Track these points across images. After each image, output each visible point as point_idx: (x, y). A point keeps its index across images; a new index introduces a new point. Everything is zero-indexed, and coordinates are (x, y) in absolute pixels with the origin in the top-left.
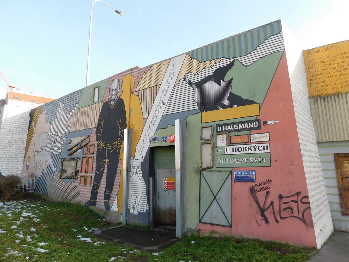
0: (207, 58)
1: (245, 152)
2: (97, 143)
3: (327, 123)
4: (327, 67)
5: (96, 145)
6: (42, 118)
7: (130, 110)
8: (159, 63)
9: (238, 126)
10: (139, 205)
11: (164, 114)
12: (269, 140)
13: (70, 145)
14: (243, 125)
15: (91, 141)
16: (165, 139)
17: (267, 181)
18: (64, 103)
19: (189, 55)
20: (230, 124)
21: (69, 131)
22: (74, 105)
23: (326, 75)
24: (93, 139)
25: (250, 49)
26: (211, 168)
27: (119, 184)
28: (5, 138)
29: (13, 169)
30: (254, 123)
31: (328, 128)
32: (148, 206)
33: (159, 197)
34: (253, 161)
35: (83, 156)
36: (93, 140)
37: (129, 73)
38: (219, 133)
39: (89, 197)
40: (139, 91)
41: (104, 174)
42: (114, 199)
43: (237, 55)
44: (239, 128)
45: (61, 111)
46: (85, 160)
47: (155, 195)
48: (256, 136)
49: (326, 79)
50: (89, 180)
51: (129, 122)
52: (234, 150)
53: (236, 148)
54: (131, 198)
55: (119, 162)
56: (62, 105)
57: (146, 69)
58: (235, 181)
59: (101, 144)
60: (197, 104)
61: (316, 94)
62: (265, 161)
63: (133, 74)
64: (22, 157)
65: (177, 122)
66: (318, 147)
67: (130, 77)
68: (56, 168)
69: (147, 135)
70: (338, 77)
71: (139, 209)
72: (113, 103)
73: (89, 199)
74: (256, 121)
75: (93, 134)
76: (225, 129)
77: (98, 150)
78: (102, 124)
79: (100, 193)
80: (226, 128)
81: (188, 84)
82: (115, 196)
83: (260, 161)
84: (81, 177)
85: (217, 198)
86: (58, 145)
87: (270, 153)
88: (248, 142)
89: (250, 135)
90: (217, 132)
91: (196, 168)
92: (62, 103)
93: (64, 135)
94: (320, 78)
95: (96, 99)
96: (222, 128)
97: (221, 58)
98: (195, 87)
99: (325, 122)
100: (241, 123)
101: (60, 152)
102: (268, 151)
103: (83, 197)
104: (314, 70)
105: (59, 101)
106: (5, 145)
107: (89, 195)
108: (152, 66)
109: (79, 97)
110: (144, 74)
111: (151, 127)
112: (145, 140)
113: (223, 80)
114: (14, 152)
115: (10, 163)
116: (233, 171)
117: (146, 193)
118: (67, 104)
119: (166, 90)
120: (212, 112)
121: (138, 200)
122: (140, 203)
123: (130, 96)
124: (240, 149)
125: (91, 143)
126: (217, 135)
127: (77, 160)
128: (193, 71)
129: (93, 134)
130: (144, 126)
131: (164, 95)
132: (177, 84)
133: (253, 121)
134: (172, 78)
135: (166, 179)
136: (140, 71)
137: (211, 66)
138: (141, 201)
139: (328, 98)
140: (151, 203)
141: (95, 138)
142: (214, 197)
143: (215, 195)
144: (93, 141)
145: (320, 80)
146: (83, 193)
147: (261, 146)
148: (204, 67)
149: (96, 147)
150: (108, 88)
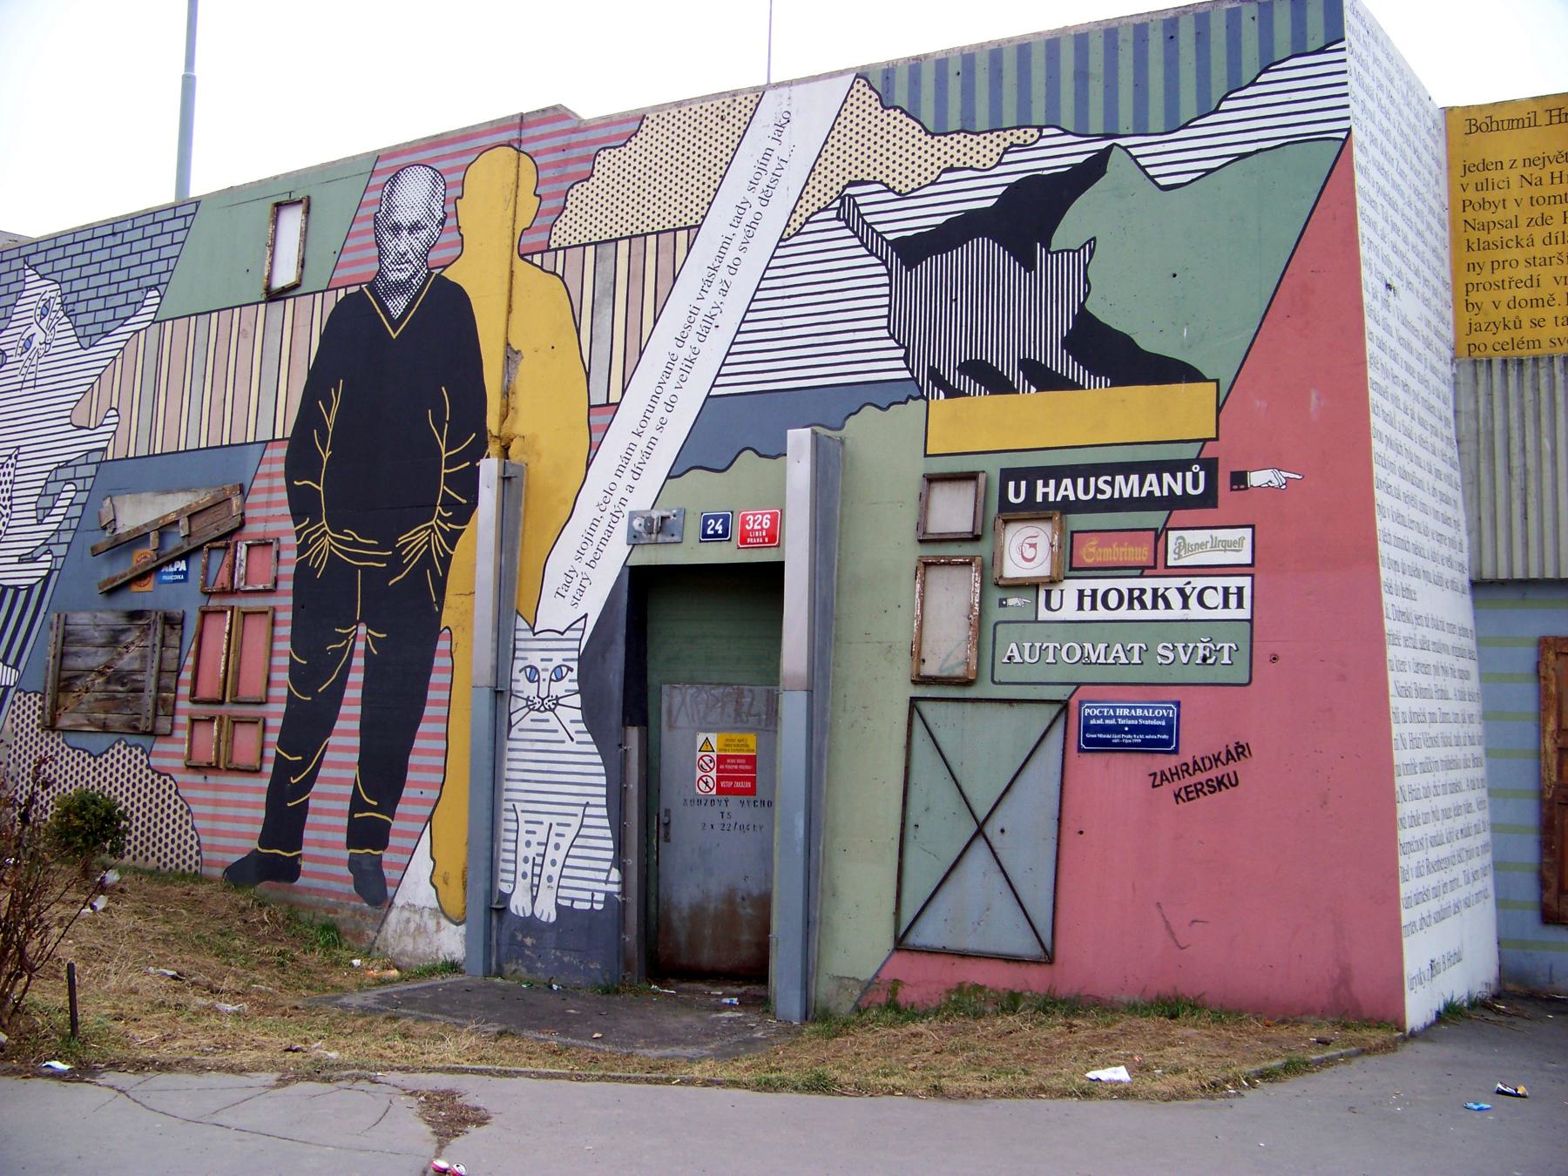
1: (1137, 613)
2: (299, 534)
3: (1525, 490)
4: (1548, 210)
5: (291, 540)
7: (511, 356)
8: (695, 107)
9: (1111, 484)
10: (566, 872)
11: (715, 391)
12: (1249, 562)
14: (1134, 478)
15: (254, 519)
16: (720, 528)
17: (1228, 752)
18: (57, 277)
19: (871, 88)
20: (1074, 472)
21: (104, 450)
23: (1539, 251)
24: (268, 504)
25: (1188, 109)
27: (440, 761)
30: (1189, 475)
31: (1525, 516)
32: (615, 875)
33: (667, 834)
34: (1171, 656)
38: (1010, 514)
39: (250, 836)
40: (565, 248)
41: (344, 710)
42: (410, 843)
43: (1125, 121)
44: (1116, 495)
48: (1193, 537)
51: (504, 417)
52: (1087, 601)
53: (1094, 592)
54: (512, 836)
55: (442, 645)
56: (38, 290)
57: (615, 130)
58: (1080, 750)
59: (325, 533)
60: (903, 351)
62: (1226, 660)
65: (799, 440)
66: (1475, 601)
67: (514, 164)
68: (15, 666)
69: (615, 499)
71: (562, 892)
72: (397, 305)
73: (255, 845)
74: (1196, 468)
75: (270, 476)
76: (1045, 495)
77: (303, 572)
78: (330, 422)
79: (319, 811)
80: (1051, 489)
81: (861, 239)
83: (1205, 659)
85: (991, 830)
87: (1251, 621)
88: (1156, 566)
89: (1166, 529)
90: (1004, 504)
92: (43, 277)
93: (67, 473)
94: (1514, 263)
96: (1031, 491)
97: (1040, 129)
99: (1516, 485)
100: (1126, 469)
101: (44, 573)
102: (1245, 613)
103: (214, 833)
104: (1485, 216)
107: (254, 820)
108: (652, 116)
109: (166, 253)
110: (597, 154)
111: (636, 457)
112: (603, 526)
113: (1046, 244)
116: (1074, 702)
117: (604, 812)
118: (80, 285)
119: (728, 260)
120: (983, 404)
121: (557, 847)
122: (569, 862)
123: (512, 272)
124: (1113, 599)
125: (254, 529)
126: (1006, 522)
128: (886, 172)
130: (593, 448)
132: (798, 234)
133: (1184, 465)
134: (765, 200)
135: (713, 738)
136: (575, 138)
137: (986, 160)
138: (573, 852)
139: (1541, 365)
140: (632, 862)
141: (279, 504)
142: (974, 828)
143: (981, 814)
146: (209, 810)
147: (1215, 589)
148: (953, 161)
149: (290, 555)
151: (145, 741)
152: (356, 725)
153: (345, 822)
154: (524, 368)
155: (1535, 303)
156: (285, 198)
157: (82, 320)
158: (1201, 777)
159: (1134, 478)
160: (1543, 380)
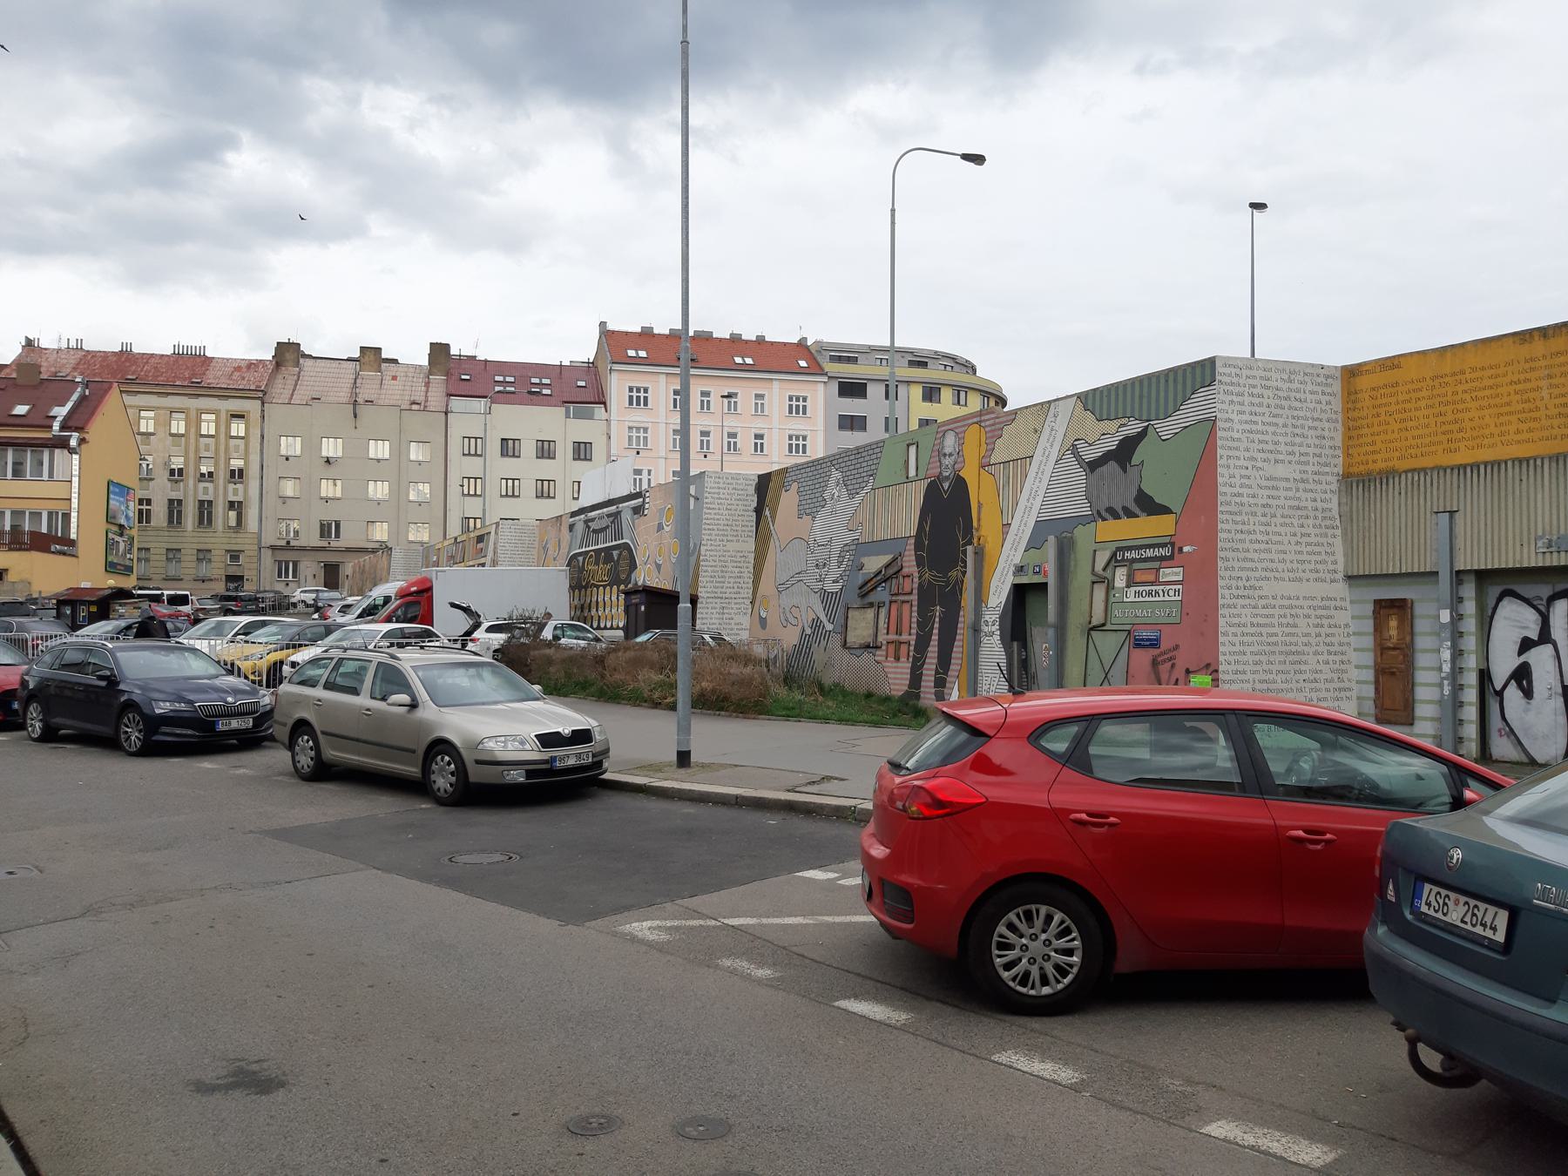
0: (1109, 414)
1: (1151, 599)
5: (916, 575)
6: (788, 502)
7: (980, 506)
9: (1145, 552)
13: (861, 572)
14: (1152, 550)
18: (841, 470)
21: (858, 539)
22: (866, 479)
23: (1376, 429)
24: (910, 561)
26: (1104, 625)
28: (712, 553)
29: (733, 626)
35: (890, 598)
36: (910, 564)
37: (975, 420)
45: (834, 490)
46: (894, 606)
47: (1027, 678)
49: (1377, 437)
50: (904, 648)
55: (961, 613)
56: (836, 475)
61: (1355, 470)
63: (983, 424)
64: (746, 596)
66: (1350, 586)
68: (833, 623)
70: (1396, 435)
72: (946, 485)
73: (906, 688)
75: (910, 550)
77: (920, 586)
78: (928, 529)
82: (953, 679)
84: (888, 643)
86: (834, 572)
88: (1156, 582)
91: (1082, 626)
93: (846, 548)
95: (912, 473)
97: (1129, 418)
98: (1088, 470)
102: (1180, 598)
103: (895, 684)
104: (1356, 414)
105: (829, 464)
106: (712, 569)
107: (906, 679)
114: (731, 585)
115: (725, 611)
118: (849, 473)
120: (1111, 522)
125: (905, 571)
126: (1116, 567)
127: (879, 607)
129: (910, 550)
130: (1004, 540)
131: (1038, 480)
138: (998, 687)
141: (912, 561)
144: (909, 567)
145: (1364, 440)
146: (892, 676)
149: (916, 580)
150: (937, 448)
151: (873, 650)
152: (936, 643)
153: (933, 679)
154: (983, 510)
155: (1374, 452)
156: (911, 442)
157: (850, 487)
158: (1166, 657)
159: (1152, 550)
160: (1372, 488)
